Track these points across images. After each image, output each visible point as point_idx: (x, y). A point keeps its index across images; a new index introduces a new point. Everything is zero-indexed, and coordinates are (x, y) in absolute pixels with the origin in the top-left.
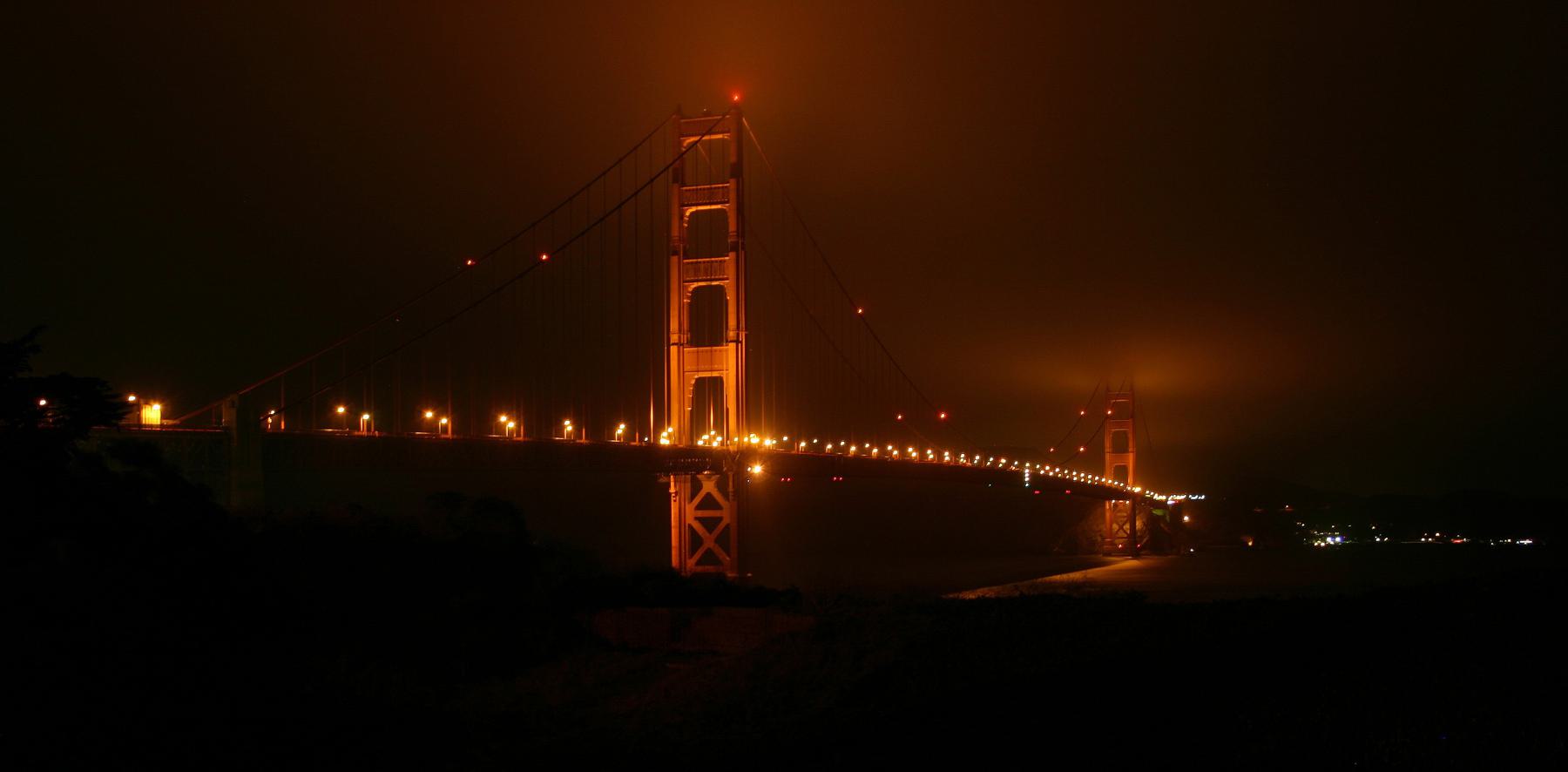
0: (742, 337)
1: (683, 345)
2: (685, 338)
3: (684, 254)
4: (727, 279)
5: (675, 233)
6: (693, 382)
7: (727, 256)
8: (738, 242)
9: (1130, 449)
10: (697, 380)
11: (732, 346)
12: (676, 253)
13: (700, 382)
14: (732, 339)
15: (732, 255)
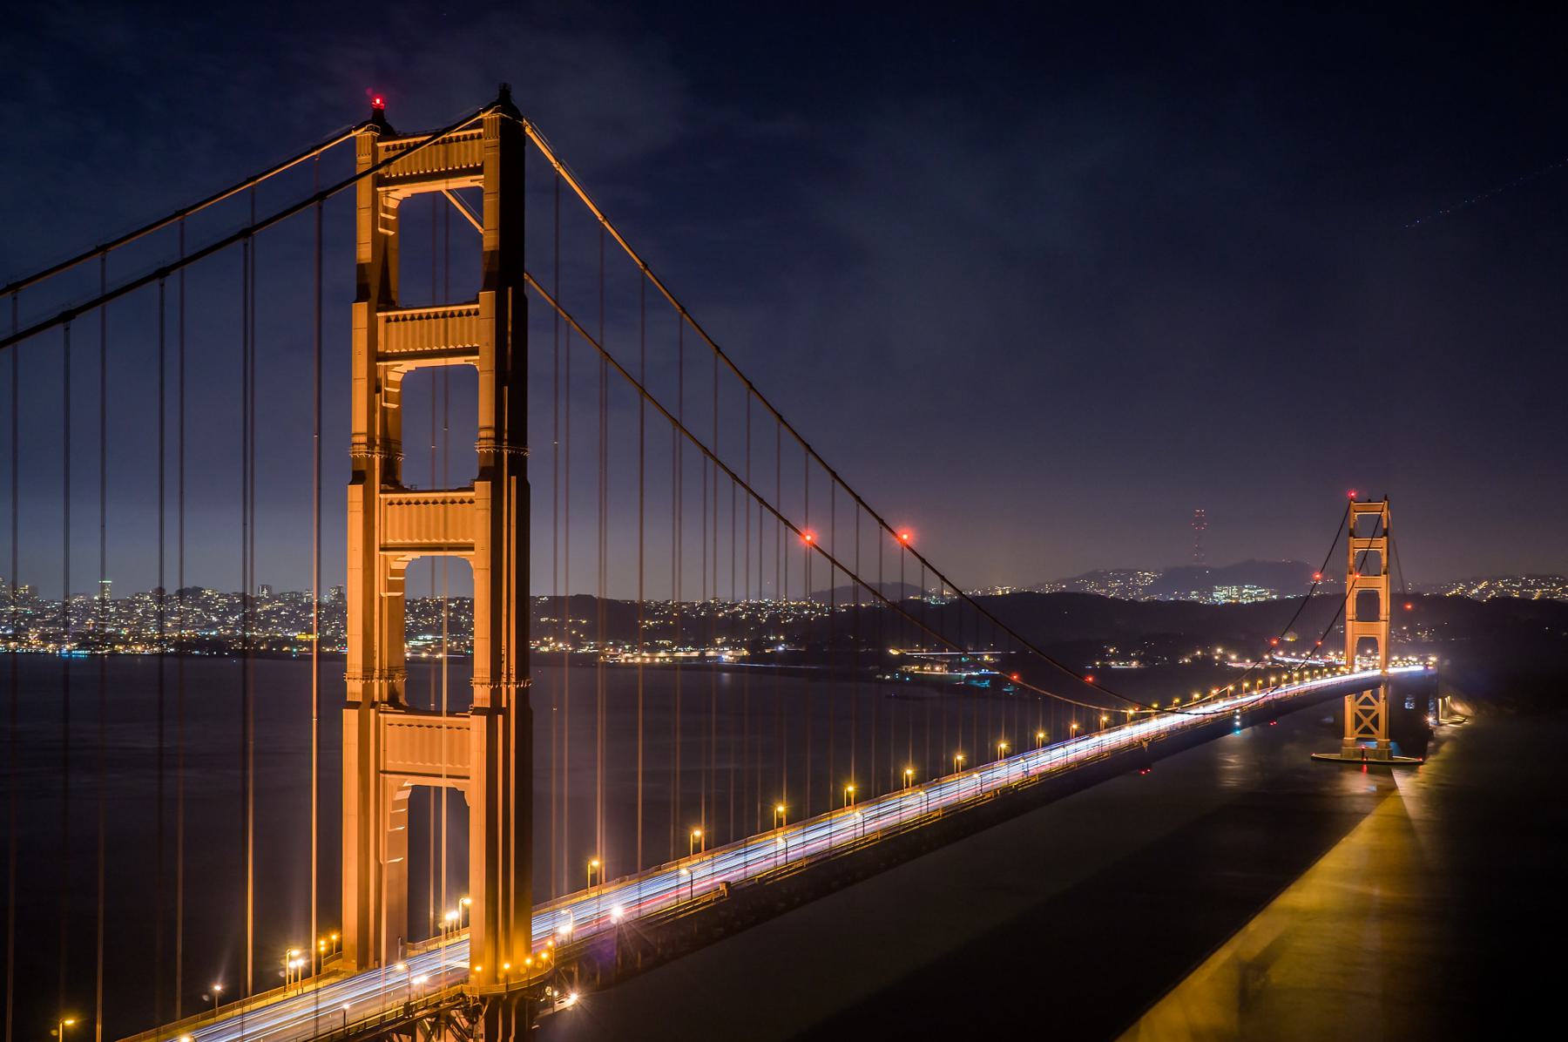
0: (510, 691)
1: (374, 705)
2: (379, 689)
3: (382, 482)
4: (471, 548)
5: (360, 423)
6: (406, 794)
7: (472, 489)
8: (498, 456)
9: (1383, 617)
10: (412, 786)
11: (478, 724)
12: (359, 477)
13: (420, 801)
14: (477, 704)
15: (483, 490)
